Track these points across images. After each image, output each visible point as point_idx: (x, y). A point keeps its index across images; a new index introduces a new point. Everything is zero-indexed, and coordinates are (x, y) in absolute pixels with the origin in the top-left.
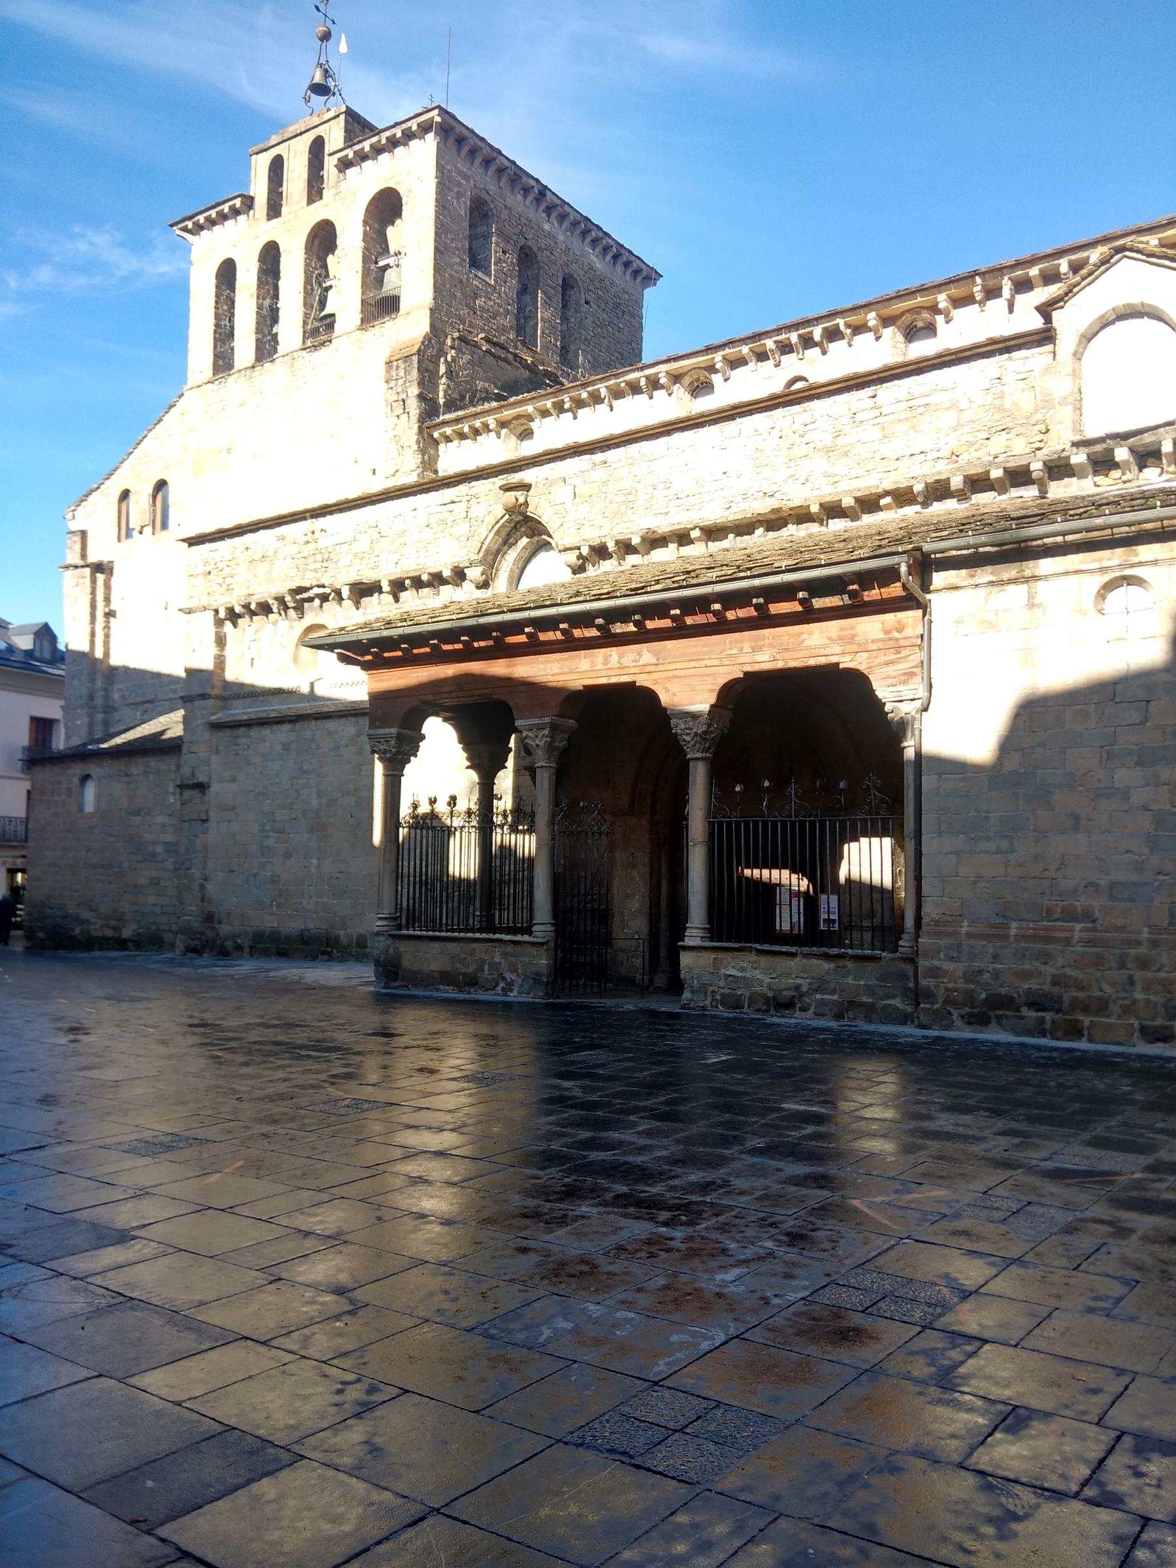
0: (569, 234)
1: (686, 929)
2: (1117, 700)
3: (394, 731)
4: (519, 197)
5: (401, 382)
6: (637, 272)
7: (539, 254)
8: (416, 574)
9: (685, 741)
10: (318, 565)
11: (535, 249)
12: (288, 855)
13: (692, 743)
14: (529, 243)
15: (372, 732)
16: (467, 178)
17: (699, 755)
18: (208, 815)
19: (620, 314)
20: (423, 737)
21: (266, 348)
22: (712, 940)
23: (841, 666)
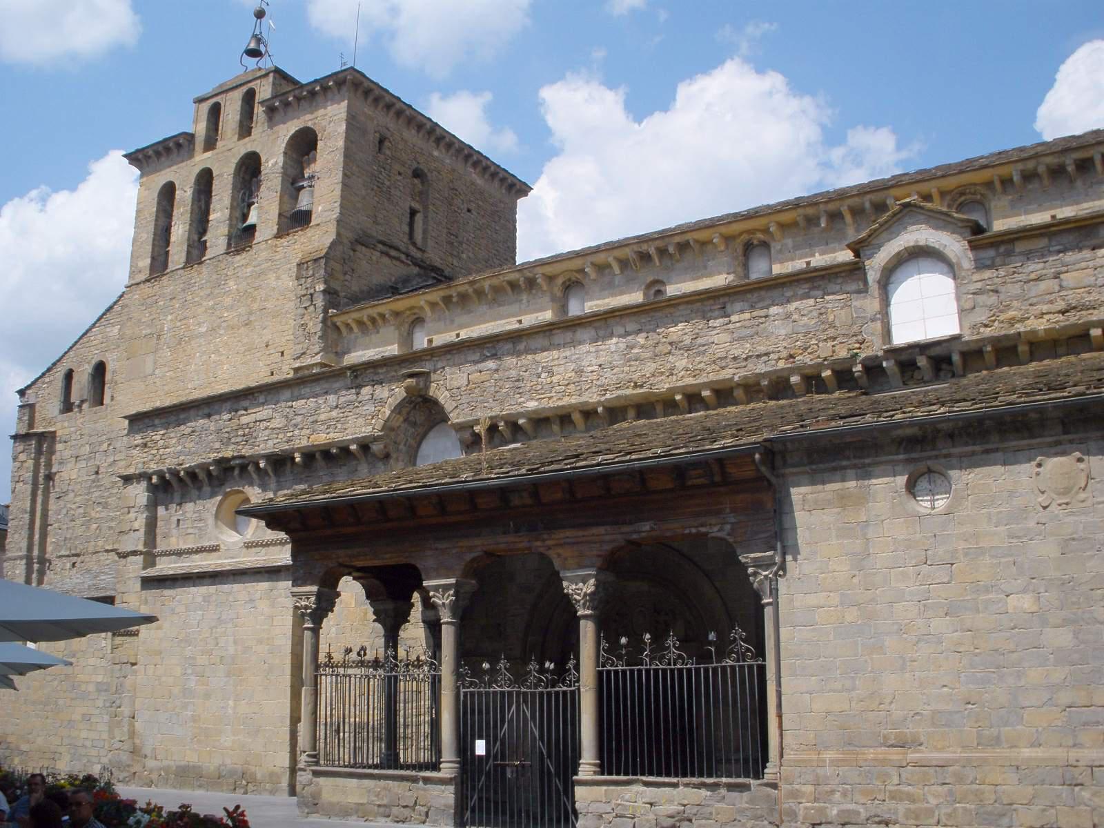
0: (454, 158)
1: (579, 765)
3: (315, 589)
4: (414, 132)
5: (309, 280)
7: (429, 174)
8: (327, 448)
9: (575, 600)
10: (239, 439)
11: (426, 171)
12: (207, 696)
13: (582, 602)
14: (421, 166)
15: (296, 589)
17: (589, 612)
18: (136, 659)
19: (497, 219)
20: (338, 595)
21: (197, 249)
22: (603, 774)
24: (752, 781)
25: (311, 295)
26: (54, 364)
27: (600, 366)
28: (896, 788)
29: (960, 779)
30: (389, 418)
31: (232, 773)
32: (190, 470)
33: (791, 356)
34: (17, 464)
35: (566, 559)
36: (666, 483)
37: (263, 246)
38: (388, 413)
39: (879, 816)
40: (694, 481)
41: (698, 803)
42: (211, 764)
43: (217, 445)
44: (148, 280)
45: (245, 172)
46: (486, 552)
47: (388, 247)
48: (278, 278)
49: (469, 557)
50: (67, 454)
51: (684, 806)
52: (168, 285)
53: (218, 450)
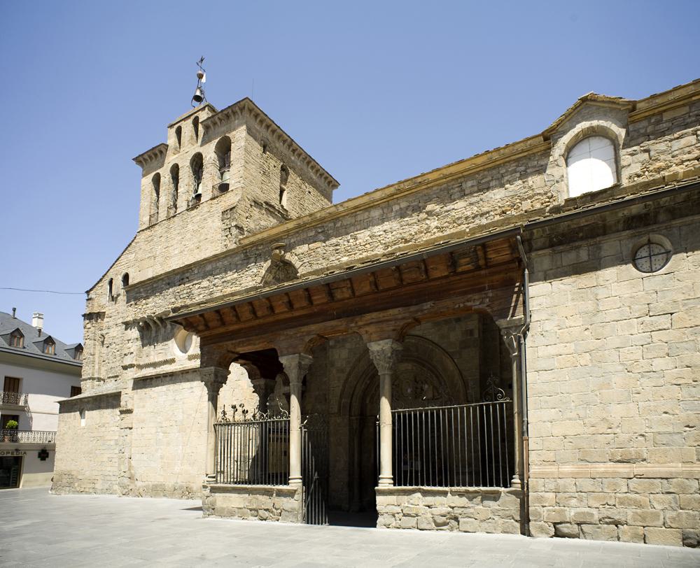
2: (651, 314)
6: (329, 183)
10: (185, 296)
16: (260, 133)
23: (473, 308)
24: (502, 489)
25: (229, 228)
26: (103, 277)
27: (385, 231)
28: (625, 495)
29: (684, 489)
30: (264, 275)
31: (181, 487)
32: (159, 316)
33: (504, 212)
34: (86, 330)
35: (371, 334)
36: (440, 271)
37: (204, 205)
38: (264, 272)
39: (610, 518)
40: (463, 267)
41: (463, 505)
42: (170, 483)
43: (173, 300)
44: (148, 228)
45: (195, 166)
46: (318, 335)
47: (269, 208)
48: (213, 221)
49: (307, 339)
50: (111, 324)
51: (453, 508)
52: (158, 230)
53: (173, 303)
